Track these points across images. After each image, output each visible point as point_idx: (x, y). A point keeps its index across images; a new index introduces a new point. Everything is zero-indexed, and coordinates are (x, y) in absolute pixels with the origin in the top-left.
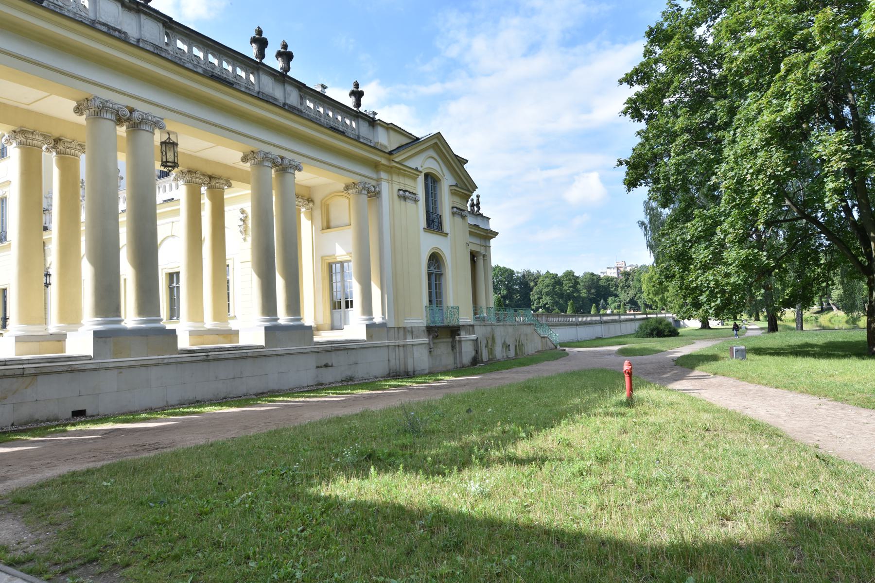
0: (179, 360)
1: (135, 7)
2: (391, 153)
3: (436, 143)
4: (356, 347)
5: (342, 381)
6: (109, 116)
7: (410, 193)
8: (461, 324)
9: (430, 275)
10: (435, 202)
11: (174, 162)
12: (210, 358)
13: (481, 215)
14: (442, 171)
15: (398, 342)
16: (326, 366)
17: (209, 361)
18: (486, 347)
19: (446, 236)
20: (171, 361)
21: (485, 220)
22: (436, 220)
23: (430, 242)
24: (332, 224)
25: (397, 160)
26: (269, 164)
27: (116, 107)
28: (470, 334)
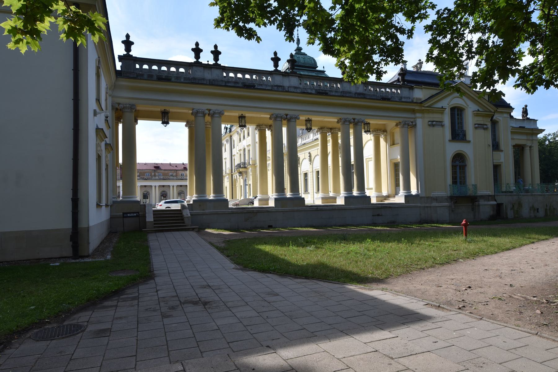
0: (305, 209)
1: (287, 74)
2: (421, 103)
4: (397, 207)
5: (388, 223)
6: (279, 119)
7: (437, 122)
8: (478, 195)
9: (454, 167)
10: (461, 123)
11: (310, 128)
12: (318, 209)
13: (528, 119)
15: (427, 205)
16: (378, 215)
17: (318, 210)
18: (511, 209)
19: (469, 143)
20: (302, 210)
21: (532, 121)
23: (458, 147)
24: (396, 142)
25: (426, 105)
26: (348, 123)
27: (281, 116)
28: (488, 201)
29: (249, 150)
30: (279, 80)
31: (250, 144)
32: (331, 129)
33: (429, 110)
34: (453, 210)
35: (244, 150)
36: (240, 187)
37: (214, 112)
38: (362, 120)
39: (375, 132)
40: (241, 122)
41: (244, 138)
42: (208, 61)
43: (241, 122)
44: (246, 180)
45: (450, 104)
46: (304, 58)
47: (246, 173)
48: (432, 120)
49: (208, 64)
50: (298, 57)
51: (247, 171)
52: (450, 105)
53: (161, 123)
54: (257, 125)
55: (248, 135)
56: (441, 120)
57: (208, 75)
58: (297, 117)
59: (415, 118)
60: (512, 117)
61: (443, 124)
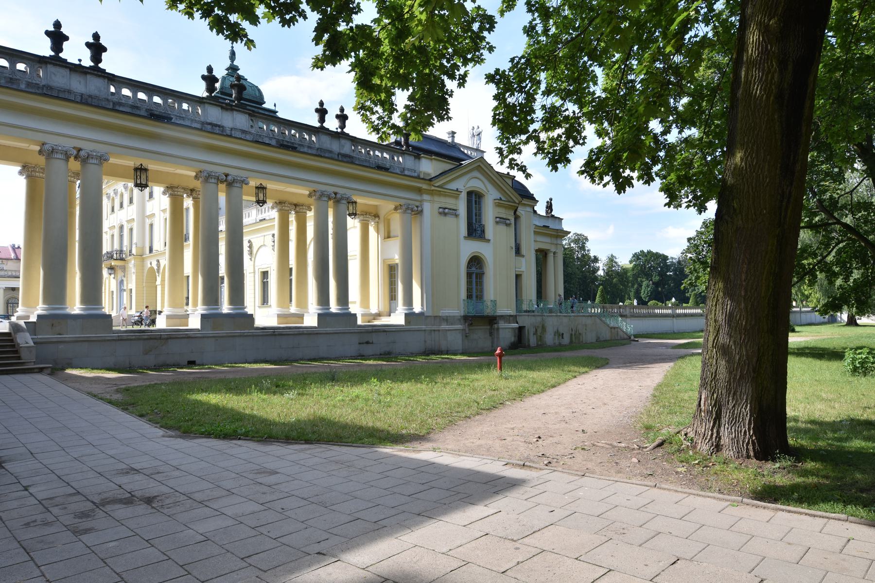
0: (254, 334)
1: (230, 107)
2: (430, 180)
3: (479, 165)
4: (394, 330)
5: (381, 354)
6: (213, 181)
7: (450, 209)
8: (498, 314)
9: (469, 275)
10: (479, 215)
11: (263, 200)
12: (276, 333)
13: (553, 216)
14: (487, 189)
15: (435, 328)
16: (367, 343)
17: (275, 335)
18: (534, 334)
20: (249, 334)
21: (557, 220)
22: (479, 229)
24: (392, 234)
25: (437, 185)
26: (326, 199)
27: (217, 175)
28: (509, 323)
29: (131, 230)
31: (134, 219)
32: (296, 205)
33: (440, 191)
34: (467, 335)
35: (121, 228)
36: (109, 293)
38: (347, 196)
39: (362, 216)
40: (139, 177)
41: (121, 206)
43: (139, 177)
44: (122, 282)
45: (467, 186)
47: (124, 269)
48: (444, 206)
51: (125, 266)
54: (167, 187)
55: (131, 201)
56: (455, 208)
57: (78, 85)
59: (421, 201)
60: (535, 212)
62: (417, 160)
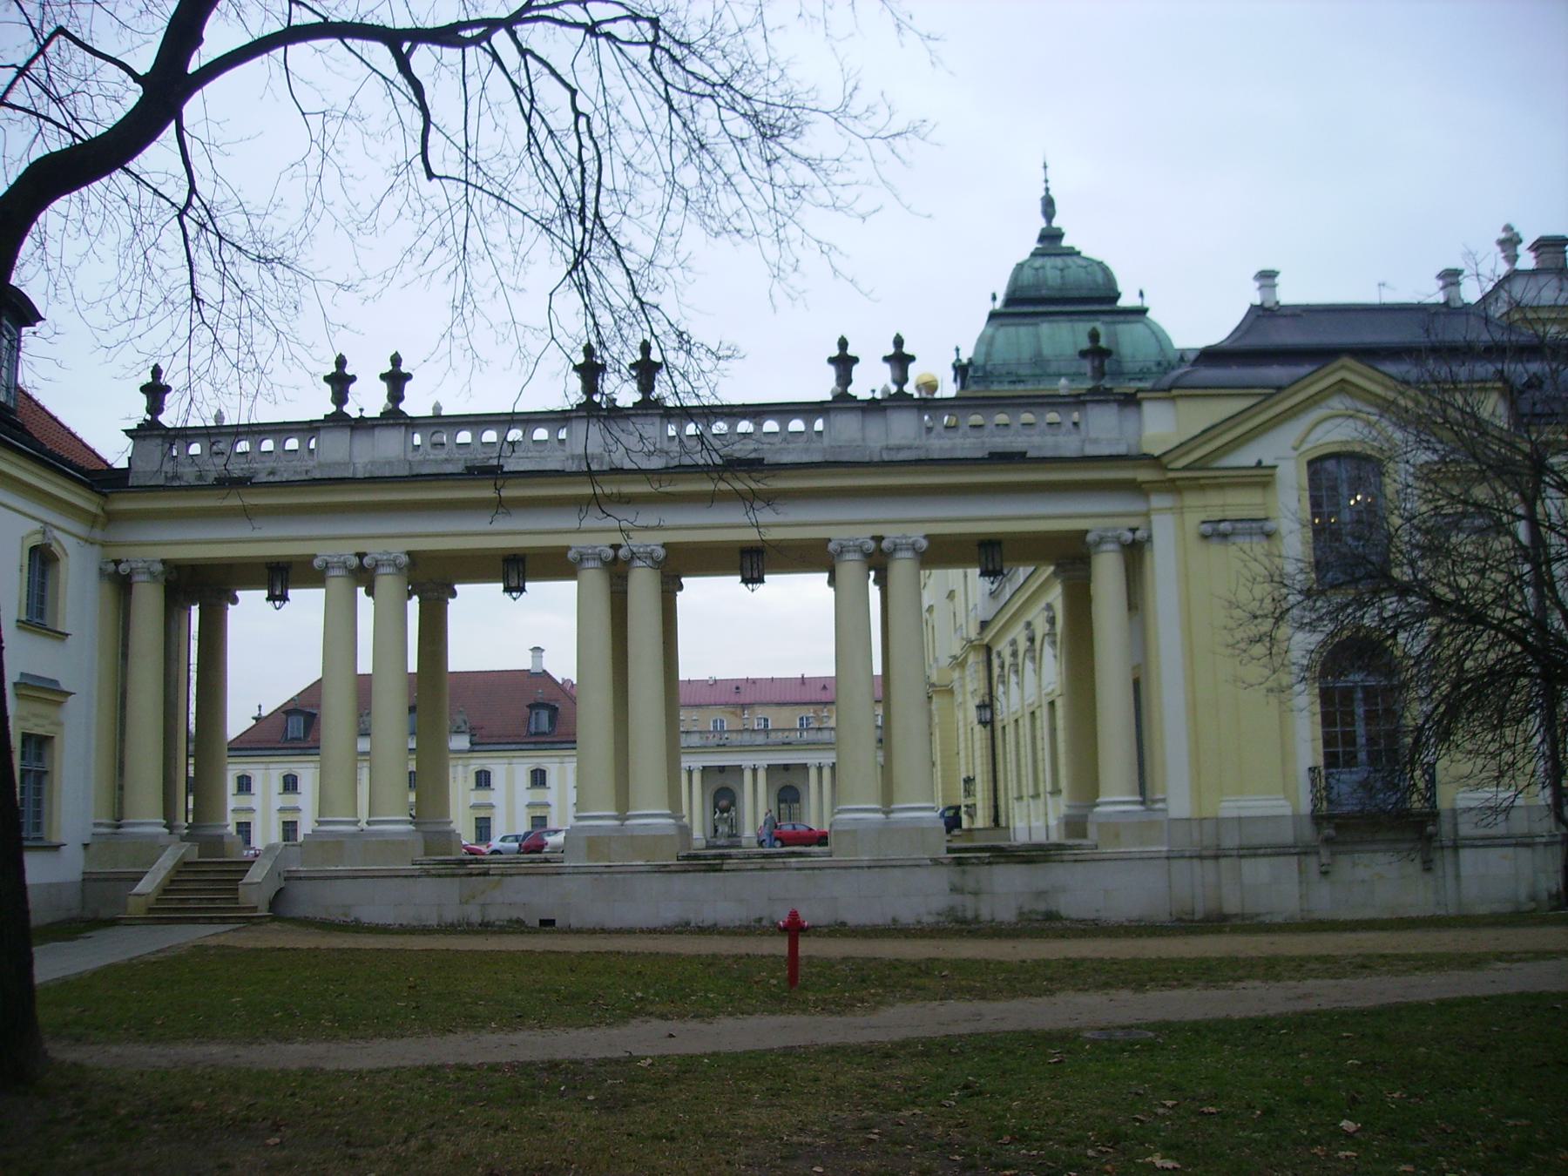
30: (590, 440)
33: (1197, 478)
37: (377, 561)
38: (910, 541)
42: (361, 410)
45: (1303, 449)
46: (1062, 270)
48: (1218, 515)
49: (361, 416)
50: (1037, 269)
52: (1304, 452)
53: (268, 599)
56: (1261, 514)
58: (653, 550)
59: (1147, 515)
61: (1268, 526)
62: (1130, 412)
